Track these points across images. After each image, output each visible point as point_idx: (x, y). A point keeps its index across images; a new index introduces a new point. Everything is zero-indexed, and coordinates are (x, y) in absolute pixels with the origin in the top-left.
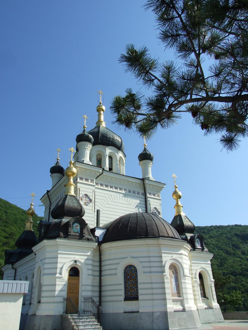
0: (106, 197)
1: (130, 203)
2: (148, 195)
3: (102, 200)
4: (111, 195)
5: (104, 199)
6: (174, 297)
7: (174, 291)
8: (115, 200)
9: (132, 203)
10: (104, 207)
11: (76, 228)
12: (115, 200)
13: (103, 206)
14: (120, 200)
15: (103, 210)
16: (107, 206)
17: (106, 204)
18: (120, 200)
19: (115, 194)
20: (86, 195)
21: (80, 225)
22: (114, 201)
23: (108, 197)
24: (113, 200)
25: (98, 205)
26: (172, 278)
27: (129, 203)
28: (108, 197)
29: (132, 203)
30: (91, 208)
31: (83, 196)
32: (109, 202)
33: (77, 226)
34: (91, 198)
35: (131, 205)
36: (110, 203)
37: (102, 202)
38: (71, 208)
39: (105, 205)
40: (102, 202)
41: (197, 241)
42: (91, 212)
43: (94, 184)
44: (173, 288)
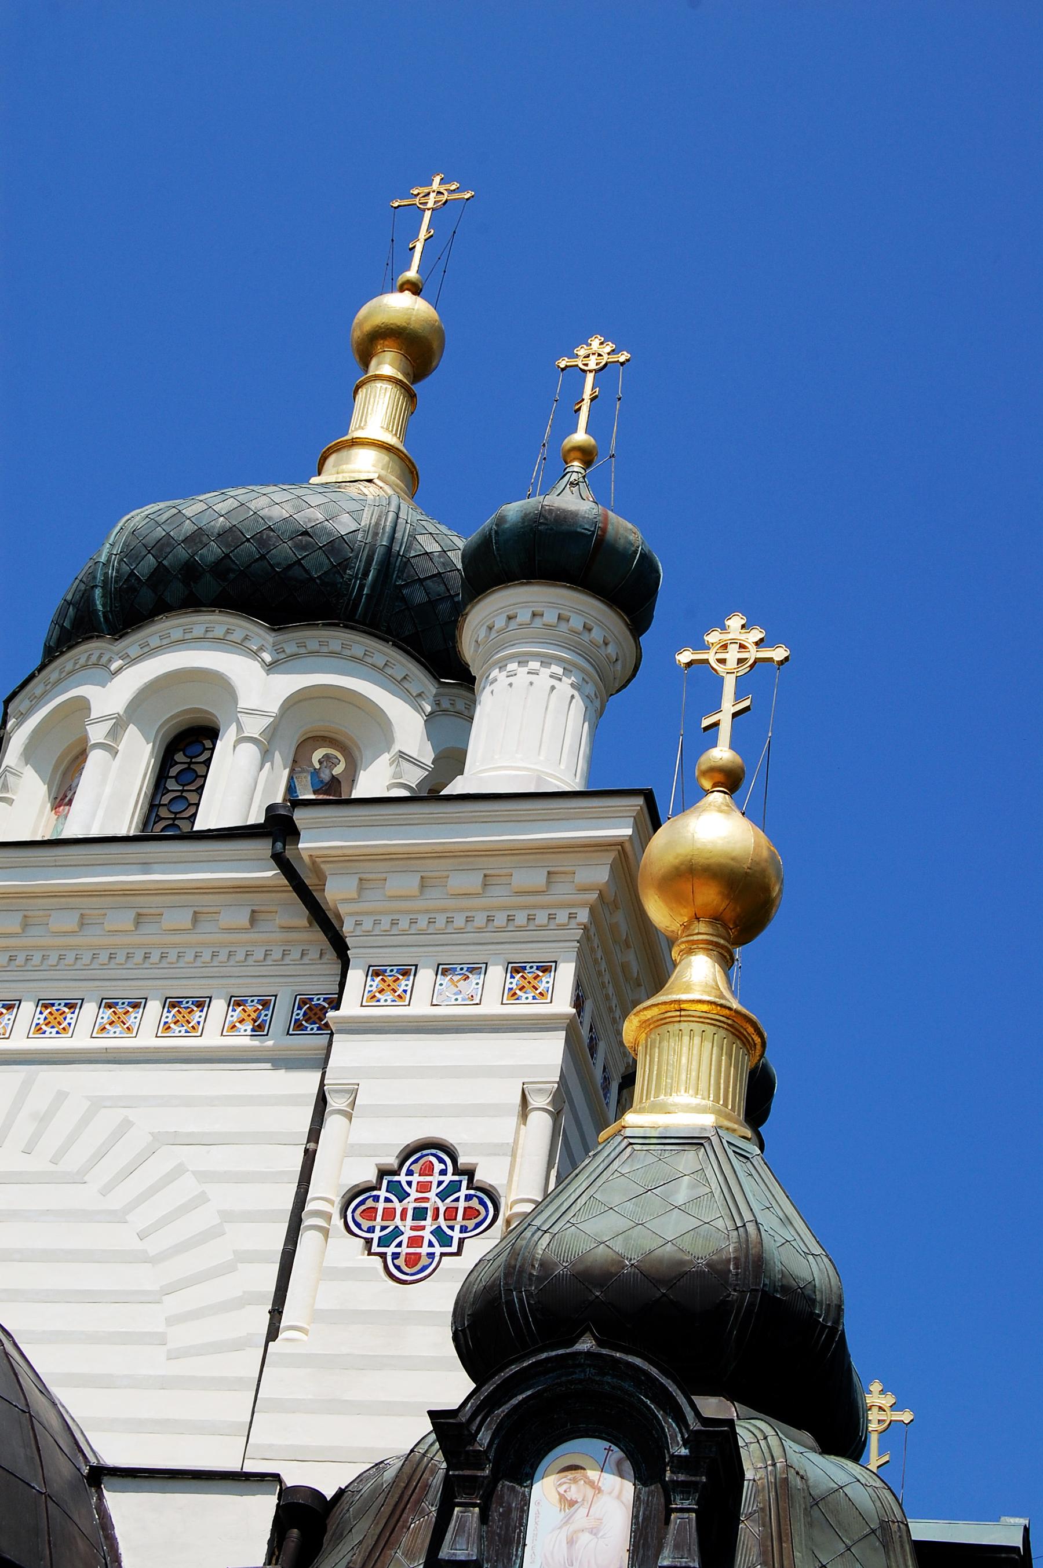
9: (100, 1155)
29: (100, 1155)
35: (78, 1179)
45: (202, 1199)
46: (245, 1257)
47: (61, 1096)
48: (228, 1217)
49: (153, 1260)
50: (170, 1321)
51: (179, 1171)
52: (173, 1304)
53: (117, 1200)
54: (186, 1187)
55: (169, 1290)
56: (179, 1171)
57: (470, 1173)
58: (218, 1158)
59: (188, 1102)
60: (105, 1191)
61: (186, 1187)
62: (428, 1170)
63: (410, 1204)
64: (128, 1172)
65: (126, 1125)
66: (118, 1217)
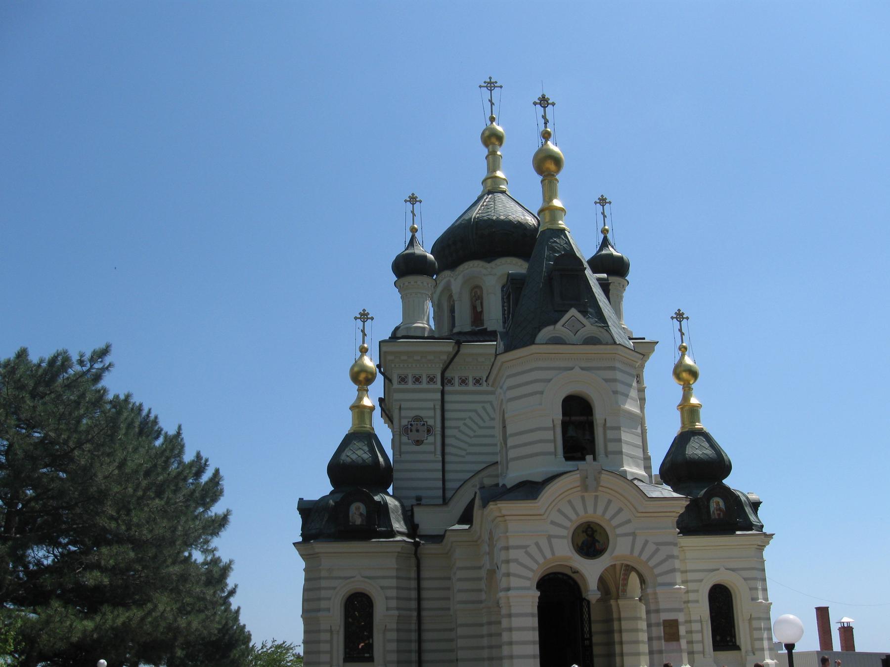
0: (476, 411)
3: (465, 419)
5: (470, 418)
10: (471, 437)
11: (357, 512)
13: (469, 436)
15: (471, 445)
17: (475, 427)
20: (418, 418)
23: (484, 408)
25: (455, 437)
28: (484, 408)
30: (432, 448)
34: (431, 422)
37: (465, 424)
40: (465, 424)
42: (431, 457)
43: (439, 386)
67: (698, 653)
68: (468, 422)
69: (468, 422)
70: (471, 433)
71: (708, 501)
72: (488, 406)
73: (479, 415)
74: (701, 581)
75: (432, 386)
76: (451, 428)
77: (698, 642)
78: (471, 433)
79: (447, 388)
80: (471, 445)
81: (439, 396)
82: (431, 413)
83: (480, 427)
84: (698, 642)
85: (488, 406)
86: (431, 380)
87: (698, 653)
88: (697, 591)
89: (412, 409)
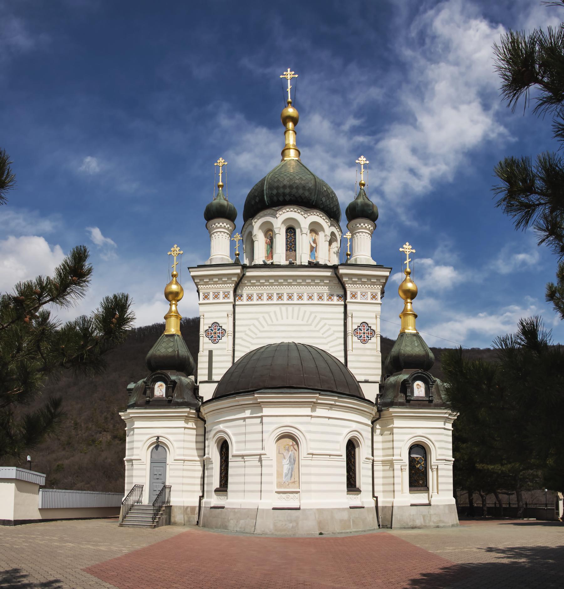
0: (257, 319)
1: (310, 322)
2: (349, 299)
4: (268, 313)
5: (254, 325)
6: (285, 488)
7: (284, 479)
8: (277, 320)
9: (313, 321)
12: (277, 320)
14: (287, 318)
15: (252, 344)
16: (260, 335)
18: (287, 318)
19: (277, 308)
21: (166, 384)
22: (275, 322)
23: (263, 317)
24: (272, 322)
25: (241, 338)
26: (285, 458)
27: (307, 322)
28: (263, 317)
29: (313, 321)
31: (209, 327)
32: (264, 327)
33: (161, 385)
35: (311, 325)
36: (267, 328)
37: (250, 329)
38: (160, 356)
39: (256, 334)
40: (250, 329)
41: (418, 385)
43: (231, 300)
44: (284, 474)
45: (330, 329)
46: (338, 338)
47: (305, 312)
48: (334, 331)
49: (326, 338)
50: (330, 347)
51: (325, 324)
52: (330, 345)
53: (317, 328)
54: (327, 327)
55: (328, 343)
56: (325, 324)
57: (370, 327)
58: (331, 322)
59: (324, 313)
60: (315, 327)
61: (327, 327)
62: (364, 327)
63: (362, 332)
64: (318, 324)
65: (316, 316)
66: (318, 331)
67: (399, 491)
68: (252, 328)
69: (252, 328)
70: (254, 336)
71: (413, 383)
72: (266, 316)
73: (259, 322)
74: (403, 441)
75: (226, 300)
76: (239, 332)
77: (398, 484)
78: (254, 336)
79: (237, 303)
80: (252, 344)
81: (231, 307)
82: (225, 320)
83: (261, 332)
84: (398, 484)
85: (266, 316)
86: (226, 296)
87: (399, 491)
88: (401, 448)
89: (212, 318)
